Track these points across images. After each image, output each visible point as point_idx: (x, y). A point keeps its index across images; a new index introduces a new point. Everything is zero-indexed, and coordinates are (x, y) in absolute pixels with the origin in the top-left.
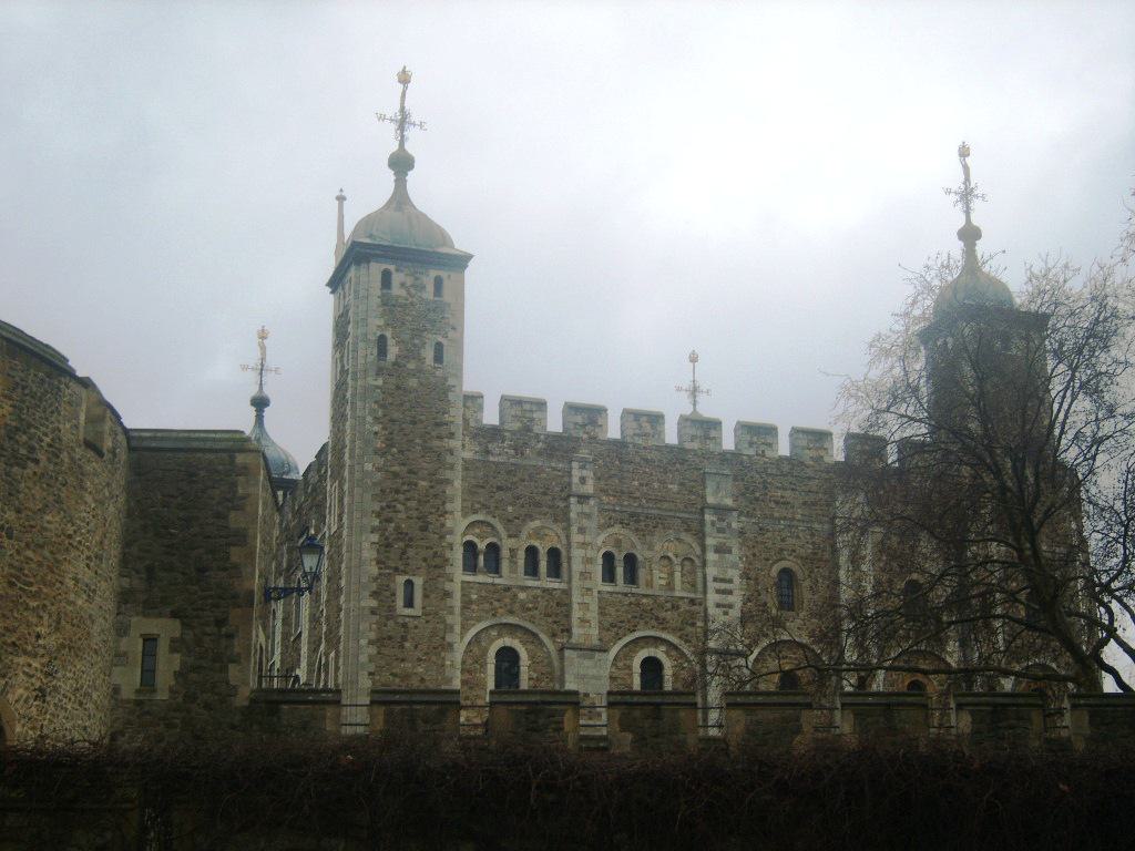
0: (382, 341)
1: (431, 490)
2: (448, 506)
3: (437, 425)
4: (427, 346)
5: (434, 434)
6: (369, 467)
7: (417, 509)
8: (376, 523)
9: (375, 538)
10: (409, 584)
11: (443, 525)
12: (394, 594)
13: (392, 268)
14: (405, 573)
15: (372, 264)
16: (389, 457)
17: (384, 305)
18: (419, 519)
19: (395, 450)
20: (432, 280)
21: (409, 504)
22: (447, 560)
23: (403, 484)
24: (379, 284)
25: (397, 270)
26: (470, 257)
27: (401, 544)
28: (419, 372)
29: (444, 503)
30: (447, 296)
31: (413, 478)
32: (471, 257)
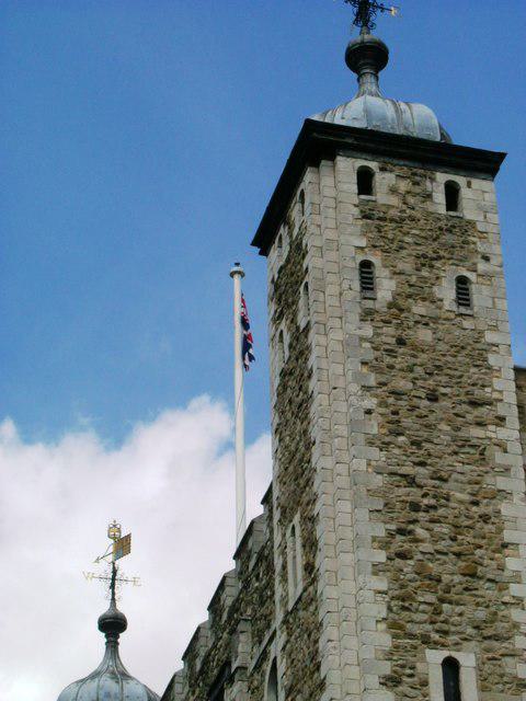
0: (366, 266)
1: (474, 509)
2: (508, 536)
3: (474, 404)
4: (444, 283)
5: (470, 417)
6: (360, 464)
7: (454, 539)
8: (381, 556)
9: (382, 583)
10: (451, 667)
11: (501, 568)
12: (425, 684)
13: (373, 165)
14: (443, 645)
15: (339, 158)
16: (396, 451)
17: (366, 216)
18: (458, 555)
19: (401, 438)
20: (442, 188)
21: (437, 528)
22: (516, 626)
23: (425, 495)
24: (355, 188)
25: (383, 169)
26: (502, 156)
27: (431, 598)
28: (435, 320)
29: (500, 530)
30: (468, 210)
31: (445, 488)
32: (502, 156)
